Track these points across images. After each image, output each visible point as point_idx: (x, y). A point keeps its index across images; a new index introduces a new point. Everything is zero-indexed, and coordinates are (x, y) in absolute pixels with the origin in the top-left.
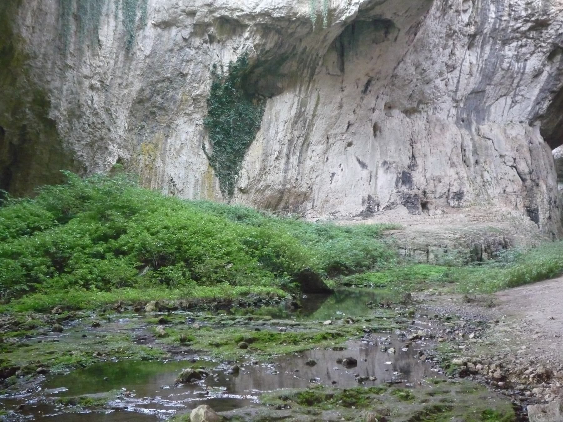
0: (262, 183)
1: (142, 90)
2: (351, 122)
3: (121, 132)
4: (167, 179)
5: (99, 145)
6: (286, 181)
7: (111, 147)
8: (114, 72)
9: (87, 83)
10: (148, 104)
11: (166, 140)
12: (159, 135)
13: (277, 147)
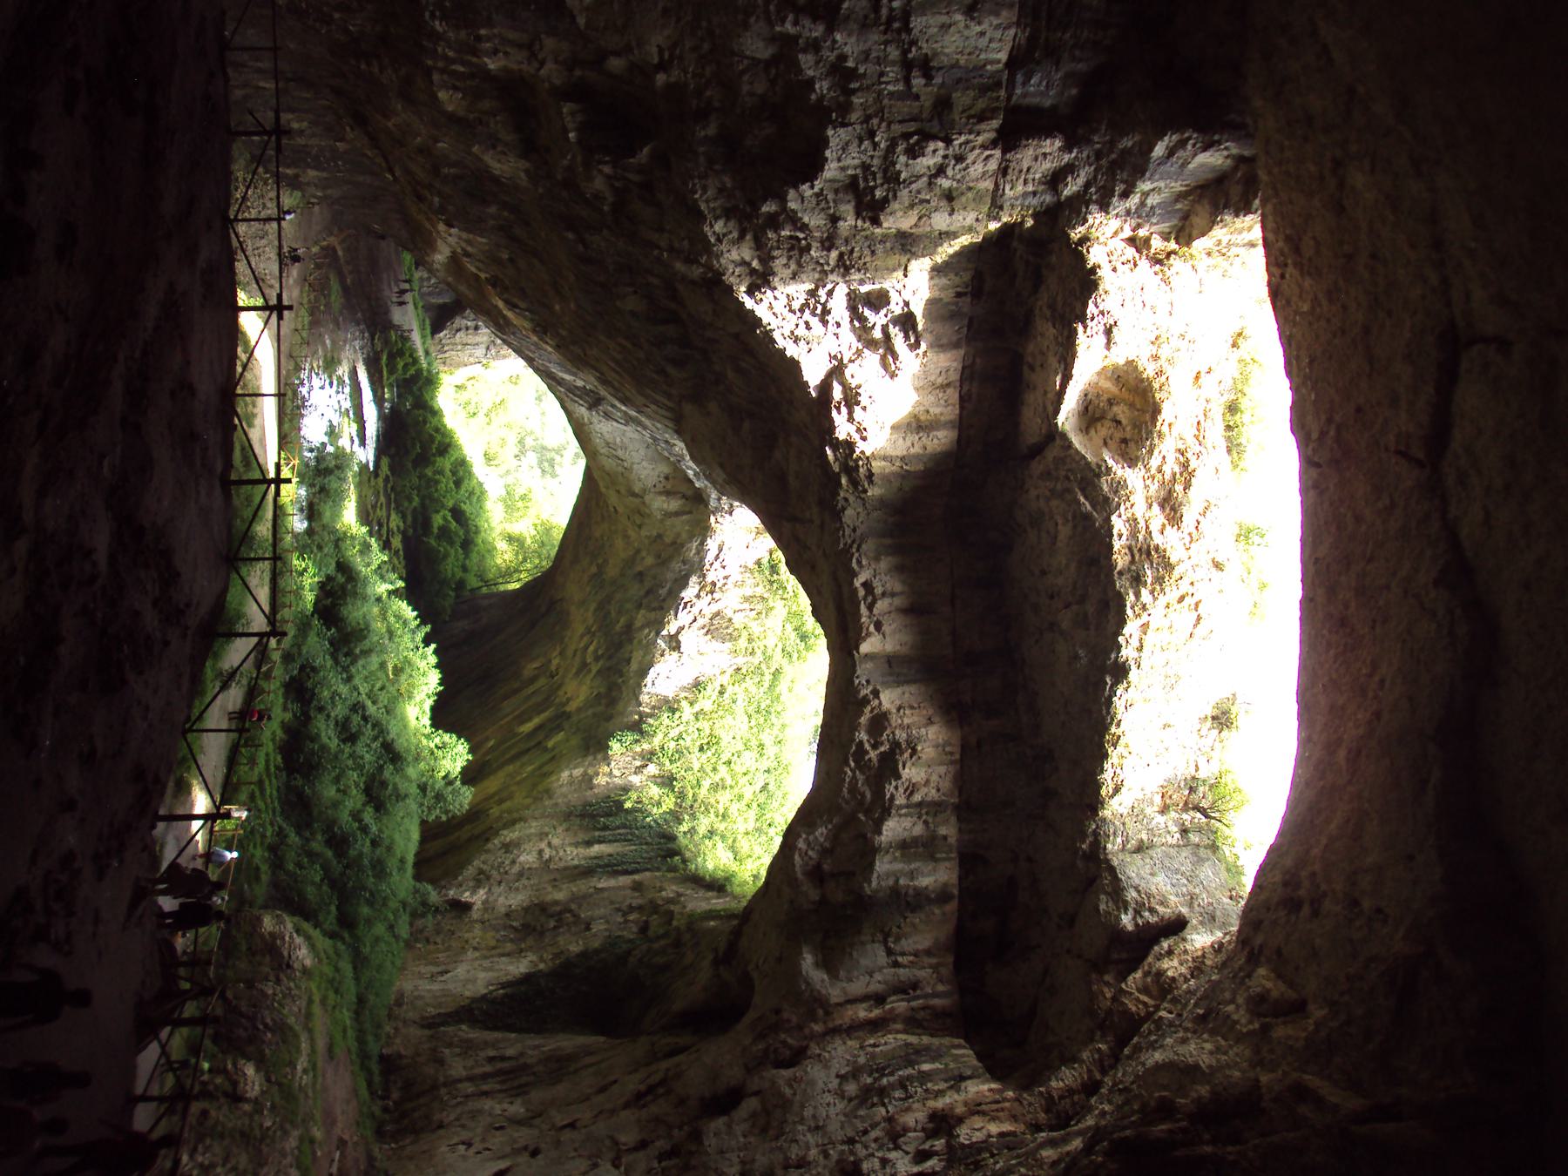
0: (447, 1051)
1: (556, 903)
2: (578, 1124)
3: (501, 900)
4: (450, 967)
5: (481, 879)
6: (452, 1083)
7: (482, 892)
8: (566, 868)
9: (543, 845)
10: (543, 919)
11: (503, 955)
12: (509, 947)
13: (510, 1052)
